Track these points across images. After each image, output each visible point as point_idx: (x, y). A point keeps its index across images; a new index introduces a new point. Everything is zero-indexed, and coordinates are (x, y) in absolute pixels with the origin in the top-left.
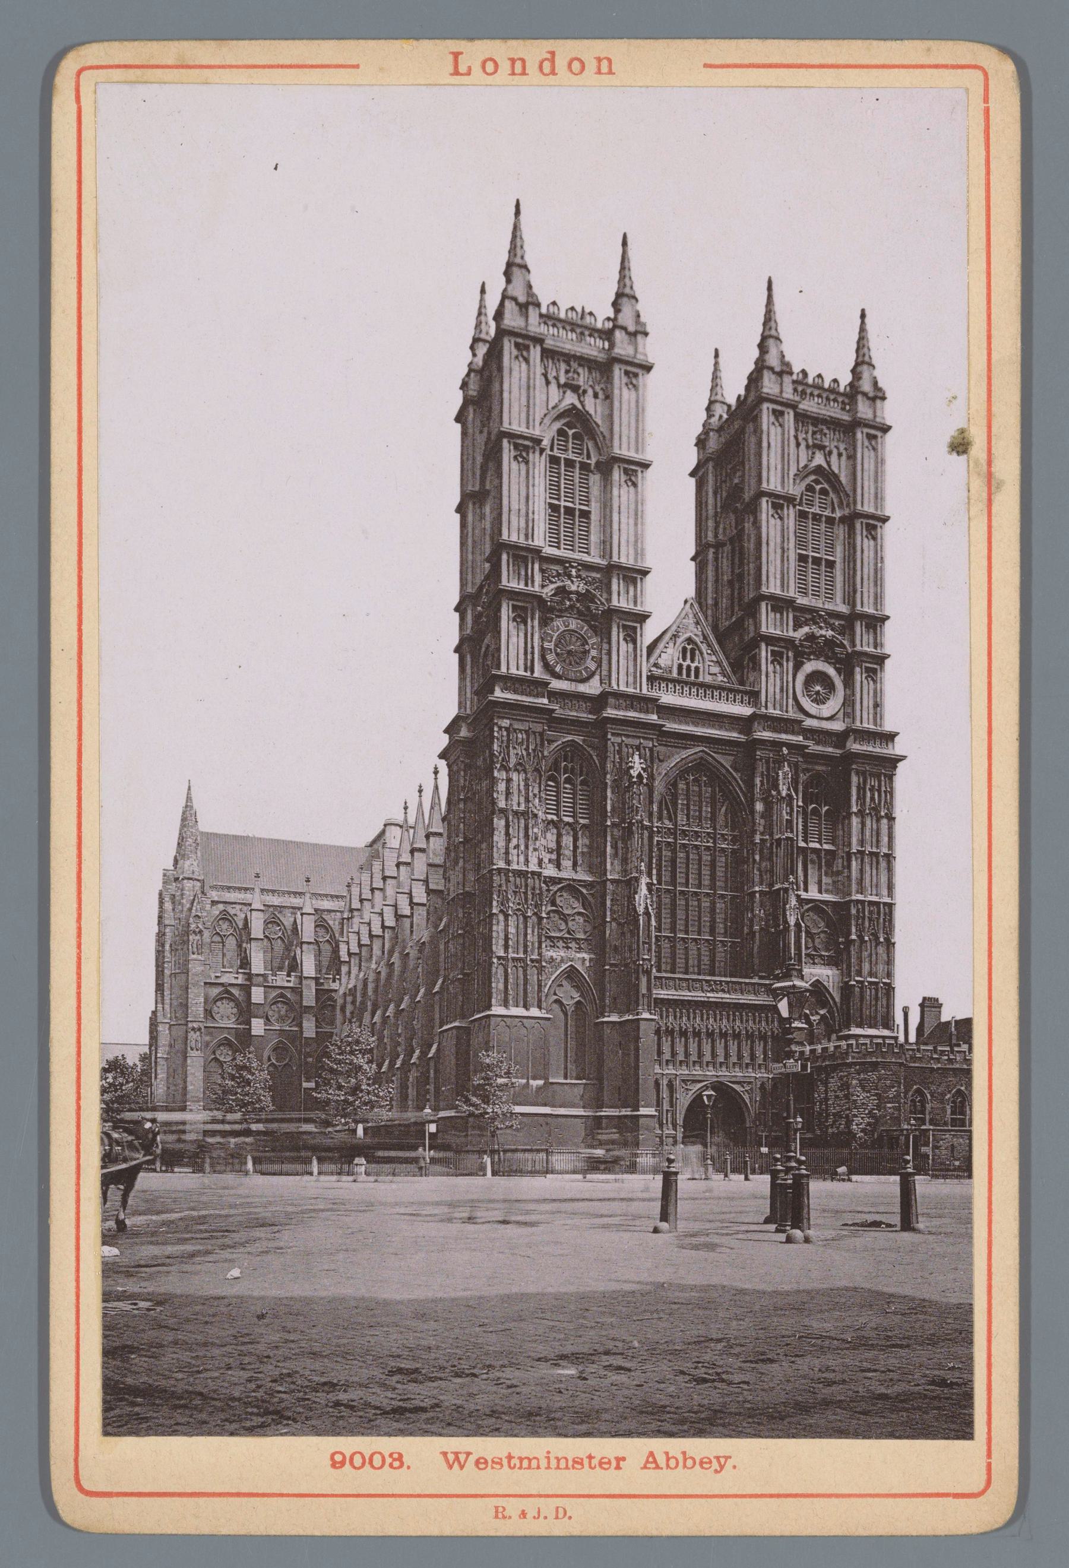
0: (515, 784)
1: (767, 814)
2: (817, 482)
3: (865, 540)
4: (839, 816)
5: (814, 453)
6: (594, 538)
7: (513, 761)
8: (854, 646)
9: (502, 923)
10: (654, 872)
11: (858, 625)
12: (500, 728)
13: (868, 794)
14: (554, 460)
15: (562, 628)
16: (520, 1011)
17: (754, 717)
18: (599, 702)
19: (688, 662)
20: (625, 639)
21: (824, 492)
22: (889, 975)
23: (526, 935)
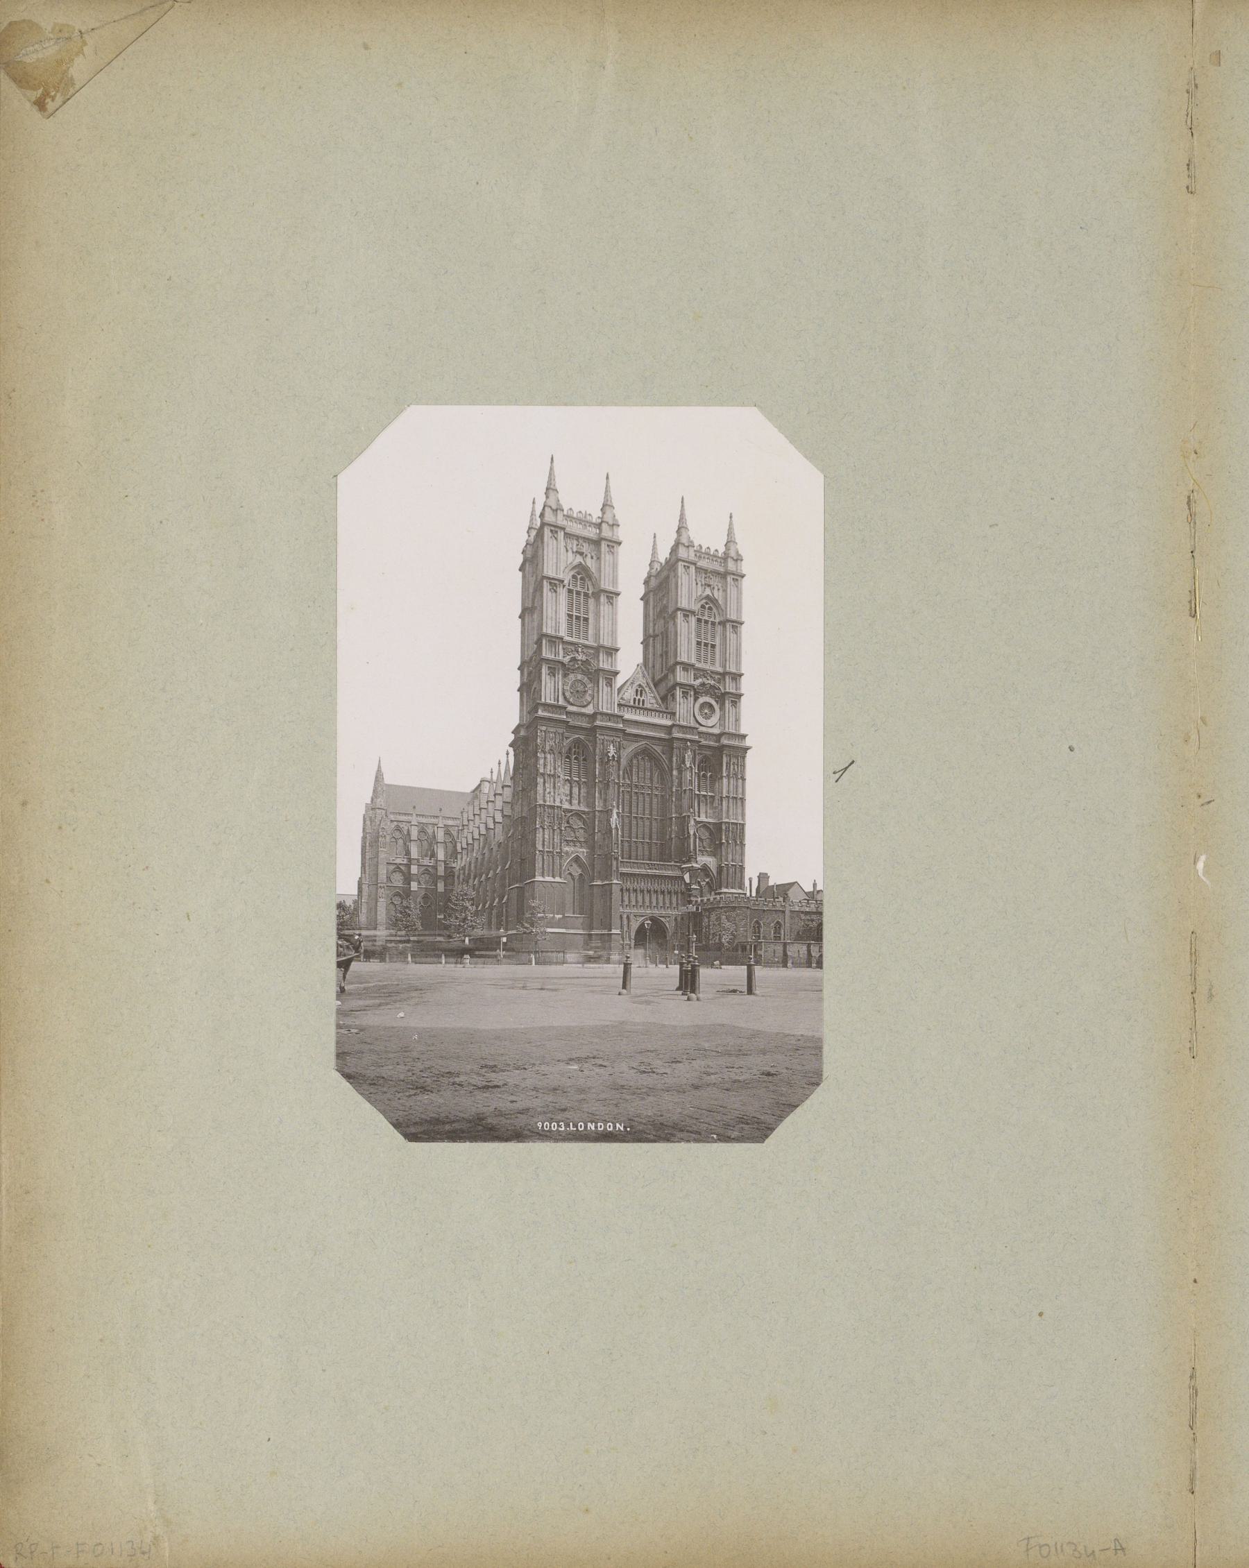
0: (548, 760)
2: (707, 603)
3: (731, 634)
4: (716, 777)
5: (705, 588)
6: (590, 632)
7: (548, 748)
8: (725, 689)
9: (541, 833)
10: (620, 806)
11: (727, 677)
12: (541, 731)
13: (732, 767)
14: (570, 591)
15: (574, 679)
17: (673, 725)
18: (593, 717)
19: (639, 697)
20: (606, 685)
21: (710, 608)
22: (742, 861)
23: (554, 839)
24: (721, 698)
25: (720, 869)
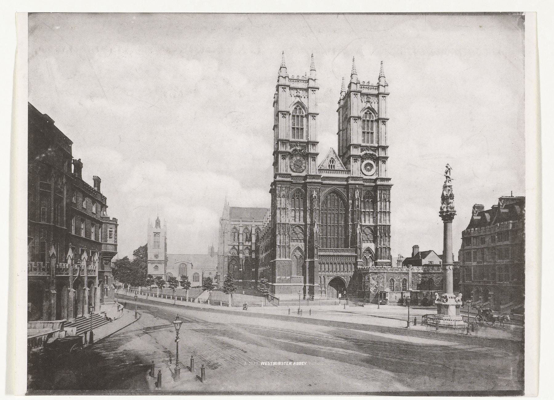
1: (353, 204)
4: (375, 202)
7: (282, 195)
8: (379, 155)
11: (380, 149)
12: (278, 187)
13: (383, 195)
14: (293, 116)
15: (296, 159)
16: (284, 259)
18: (305, 177)
19: (332, 164)
20: (312, 160)
21: (370, 114)
22: (389, 245)
23: (285, 239)
24: (377, 160)
25: (377, 249)
